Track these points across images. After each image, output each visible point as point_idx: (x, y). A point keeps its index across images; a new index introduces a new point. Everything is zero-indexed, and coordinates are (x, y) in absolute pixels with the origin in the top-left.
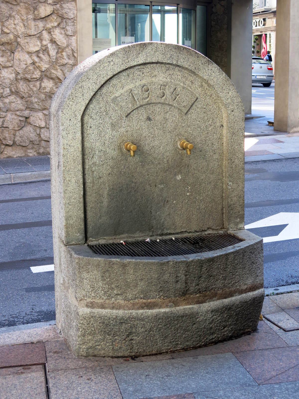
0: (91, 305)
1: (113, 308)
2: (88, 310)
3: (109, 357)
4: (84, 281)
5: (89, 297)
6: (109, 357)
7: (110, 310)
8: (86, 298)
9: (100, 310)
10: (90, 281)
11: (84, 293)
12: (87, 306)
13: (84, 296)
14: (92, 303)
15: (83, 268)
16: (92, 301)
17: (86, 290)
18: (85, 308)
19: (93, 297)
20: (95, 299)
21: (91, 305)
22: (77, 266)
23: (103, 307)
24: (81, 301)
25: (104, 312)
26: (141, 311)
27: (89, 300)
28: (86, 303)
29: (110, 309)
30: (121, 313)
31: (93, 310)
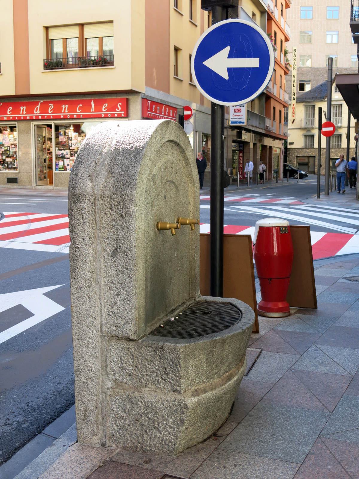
0: (195, 393)
1: (212, 389)
2: (195, 399)
3: (199, 443)
4: (189, 370)
5: (193, 385)
6: (199, 443)
7: (210, 393)
8: (190, 388)
9: (204, 395)
10: (195, 368)
11: (188, 382)
12: (193, 395)
13: (188, 387)
14: (196, 391)
15: (189, 356)
16: (196, 388)
17: (190, 379)
18: (192, 398)
19: (197, 384)
20: (199, 385)
21: (196, 393)
22: (183, 356)
23: (205, 391)
24: (186, 392)
25: (208, 395)
26: (227, 385)
27: (193, 388)
28: (191, 393)
29: (211, 391)
30: (217, 392)
31: (199, 397)
